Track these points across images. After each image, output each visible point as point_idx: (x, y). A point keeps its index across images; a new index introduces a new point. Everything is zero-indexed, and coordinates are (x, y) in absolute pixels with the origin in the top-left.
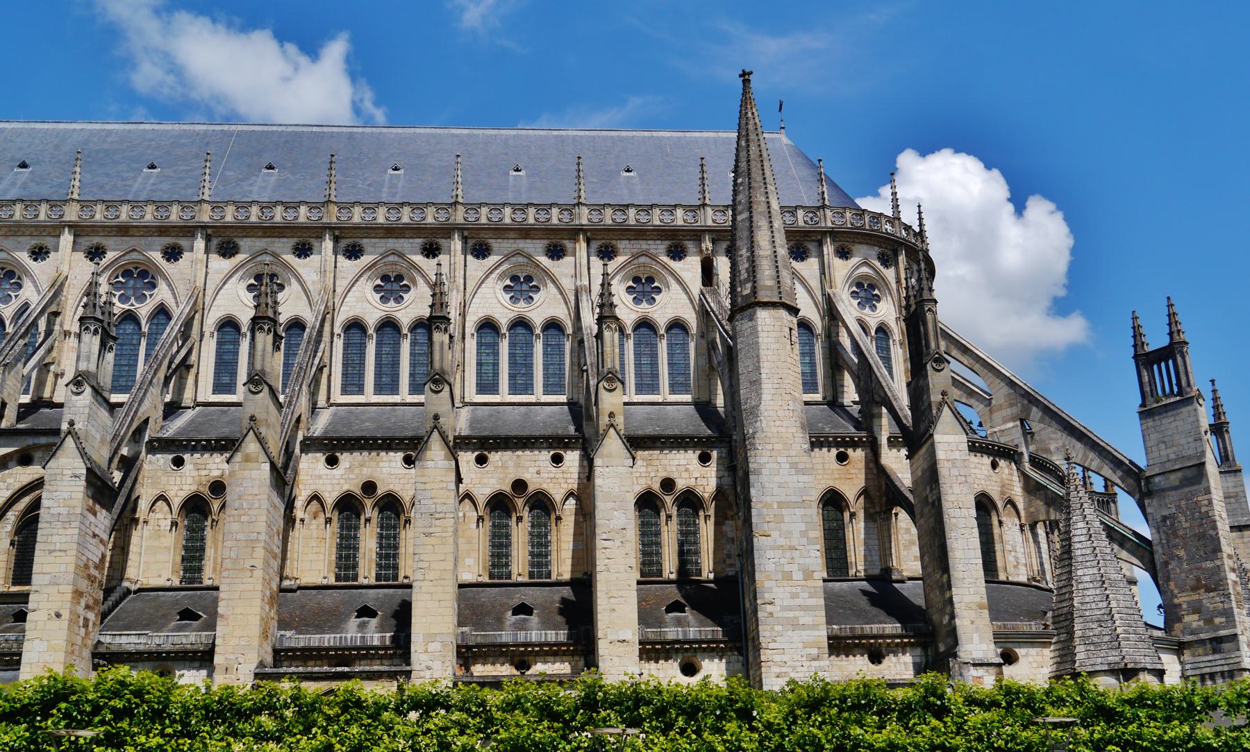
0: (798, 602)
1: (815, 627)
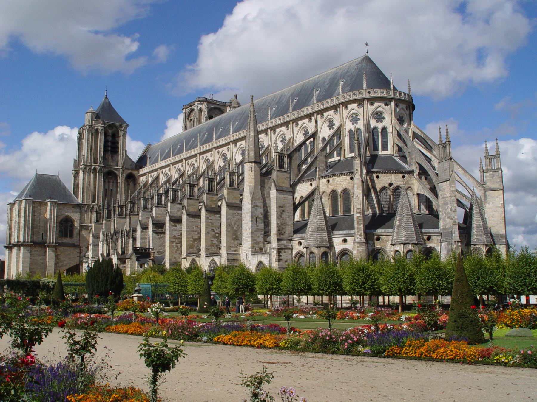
0: (247, 236)
1: (250, 241)
